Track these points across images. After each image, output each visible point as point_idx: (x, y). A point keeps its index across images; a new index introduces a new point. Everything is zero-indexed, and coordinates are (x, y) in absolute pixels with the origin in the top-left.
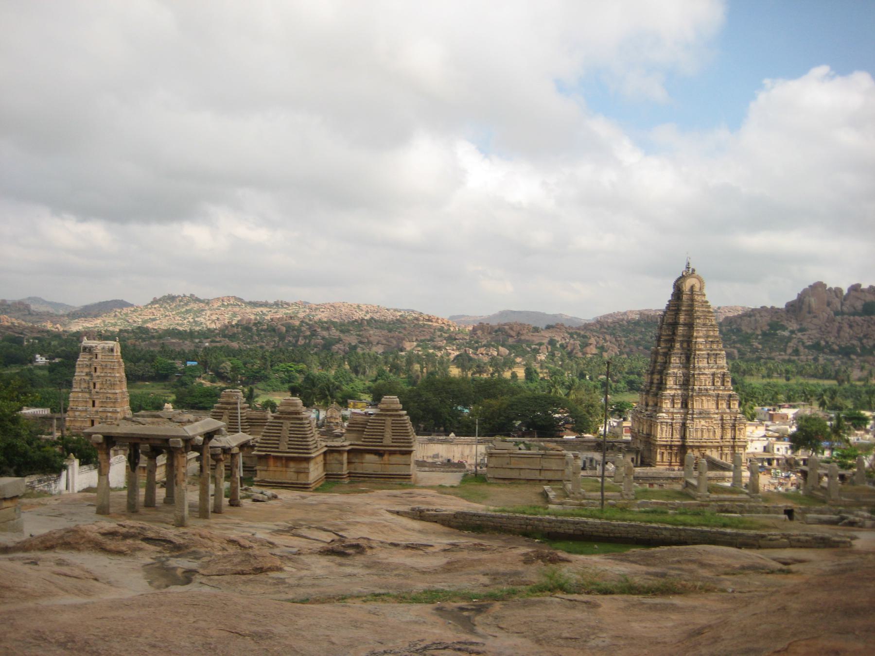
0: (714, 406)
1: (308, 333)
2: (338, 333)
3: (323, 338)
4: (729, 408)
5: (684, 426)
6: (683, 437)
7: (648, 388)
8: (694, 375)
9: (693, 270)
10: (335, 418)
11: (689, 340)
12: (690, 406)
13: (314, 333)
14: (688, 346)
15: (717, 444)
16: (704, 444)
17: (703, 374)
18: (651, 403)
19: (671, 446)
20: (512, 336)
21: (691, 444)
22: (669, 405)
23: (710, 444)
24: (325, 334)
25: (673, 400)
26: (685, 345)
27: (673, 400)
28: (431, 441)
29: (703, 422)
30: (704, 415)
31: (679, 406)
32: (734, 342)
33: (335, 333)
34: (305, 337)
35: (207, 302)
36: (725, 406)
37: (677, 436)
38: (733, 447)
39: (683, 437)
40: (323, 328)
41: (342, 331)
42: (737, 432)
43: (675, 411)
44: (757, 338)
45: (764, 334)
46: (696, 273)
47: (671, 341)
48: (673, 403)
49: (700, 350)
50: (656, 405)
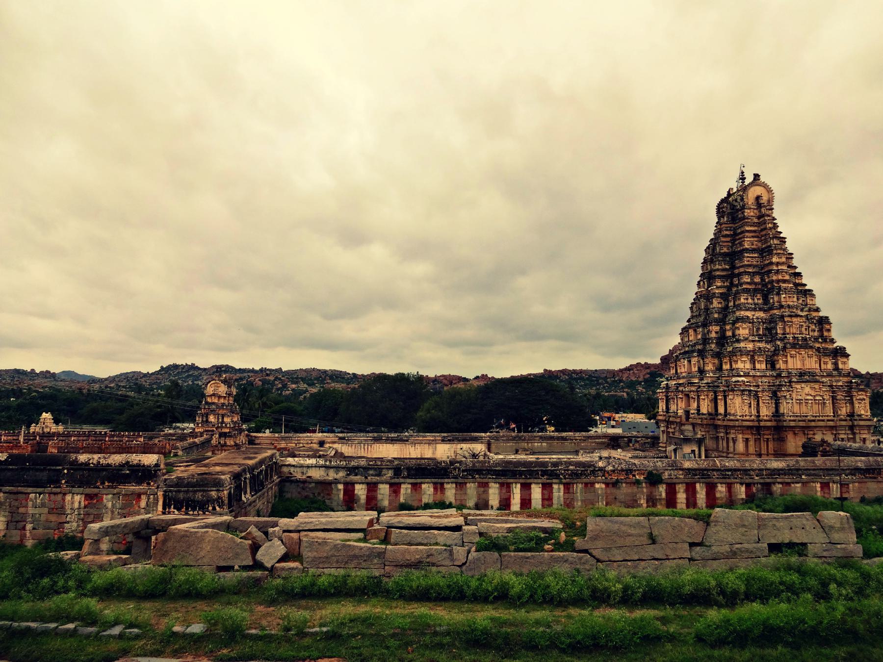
0: (817, 366)
1: (280, 386)
2: (306, 386)
3: (293, 390)
4: (836, 368)
5: (776, 397)
6: (777, 414)
7: (700, 347)
8: (782, 317)
9: (757, 177)
10: (220, 397)
11: (763, 271)
12: (781, 365)
13: (285, 386)
14: (762, 280)
15: (831, 424)
16: (813, 424)
17: (797, 316)
18: (710, 367)
19: (758, 428)
20: (447, 385)
21: (792, 424)
22: (748, 366)
23: (822, 424)
24: (294, 386)
25: (753, 358)
26: (757, 279)
27: (753, 358)
28: (377, 440)
29: (807, 389)
30: (805, 376)
31: (763, 366)
32: (623, 388)
33: (303, 386)
34: (278, 389)
35: (205, 369)
36: (830, 366)
37: (766, 411)
38: (852, 428)
39: (777, 414)
40: (293, 383)
41: (309, 385)
42: (857, 405)
43: (758, 374)
44: (640, 383)
45: (646, 381)
46: (762, 179)
47: (731, 276)
48: (753, 361)
49: (785, 281)
50: (720, 369)
